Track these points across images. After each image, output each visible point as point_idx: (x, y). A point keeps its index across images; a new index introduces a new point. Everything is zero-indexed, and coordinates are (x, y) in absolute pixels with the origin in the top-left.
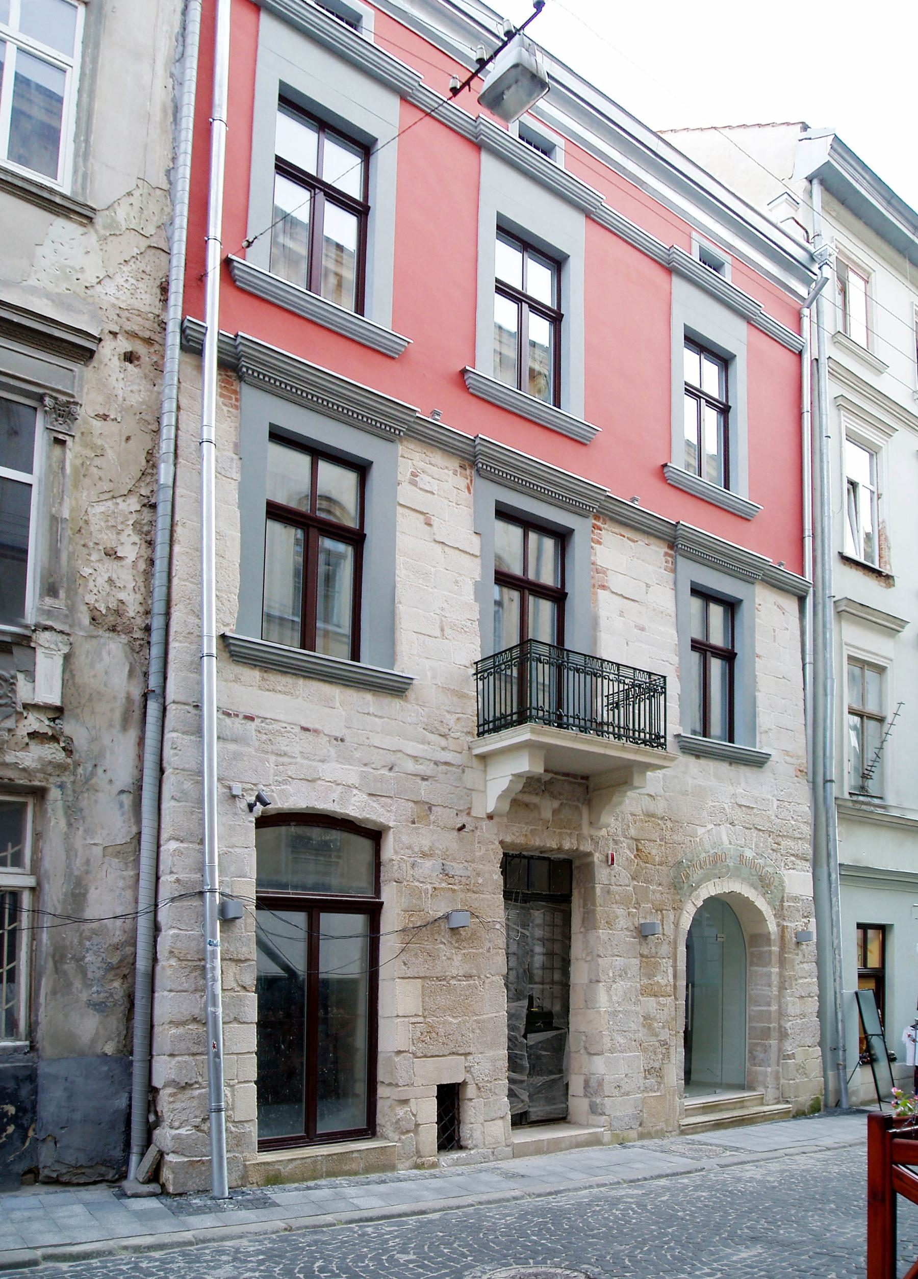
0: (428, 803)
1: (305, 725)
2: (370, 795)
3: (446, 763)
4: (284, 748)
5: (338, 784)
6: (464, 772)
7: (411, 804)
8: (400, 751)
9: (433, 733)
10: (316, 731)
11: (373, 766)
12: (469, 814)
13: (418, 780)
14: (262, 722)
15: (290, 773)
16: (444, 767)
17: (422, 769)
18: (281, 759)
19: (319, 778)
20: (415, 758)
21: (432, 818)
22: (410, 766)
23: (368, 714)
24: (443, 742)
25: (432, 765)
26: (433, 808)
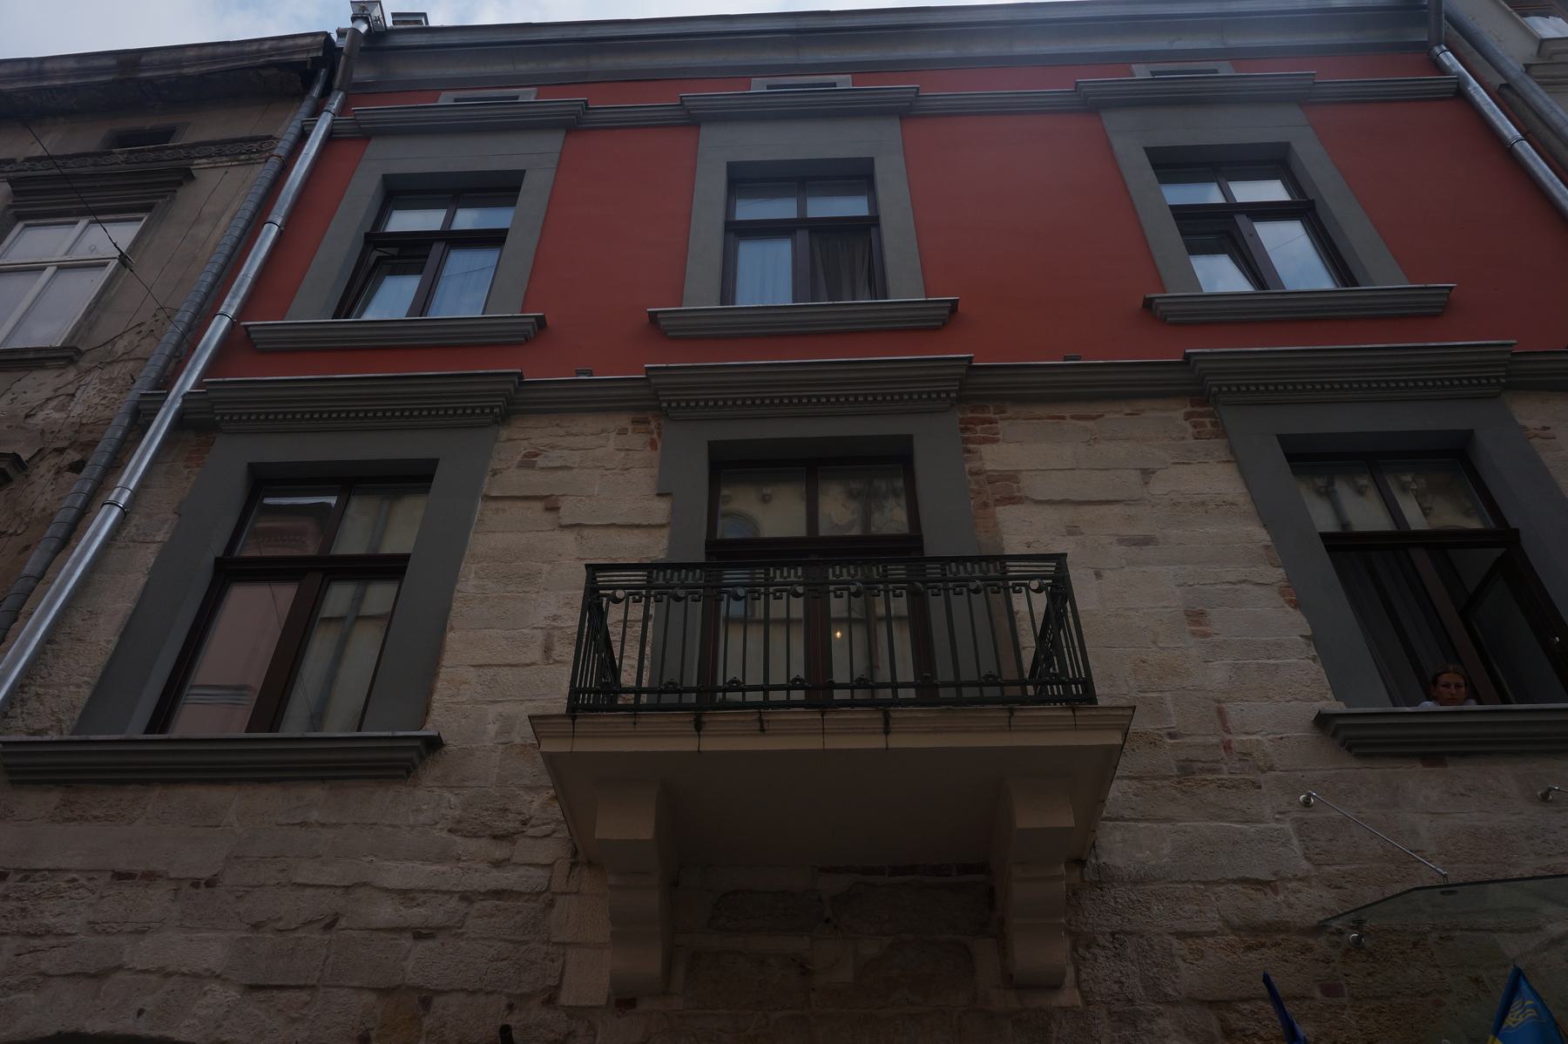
0: (420, 989)
1: (123, 867)
2: (254, 988)
3: (498, 894)
4: (49, 920)
5: (169, 975)
6: (551, 904)
7: (369, 998)
8: (365, 884)
9: (475, 836)
10: (150, 876)
11: (280, 925)
12: (550, 1001)
13: (406, 942)
14: (26, 878)
15: (44, 966)
16: (489, 904)
17: (416, 915)
18: (36, 942)
19: (119, 968)
20: (406, 895)
21: (428, 1022)
22: (387, 912)
23: (303, 824)
24: (500, 851)
25: (453, 903)
26: (438, 1001)
